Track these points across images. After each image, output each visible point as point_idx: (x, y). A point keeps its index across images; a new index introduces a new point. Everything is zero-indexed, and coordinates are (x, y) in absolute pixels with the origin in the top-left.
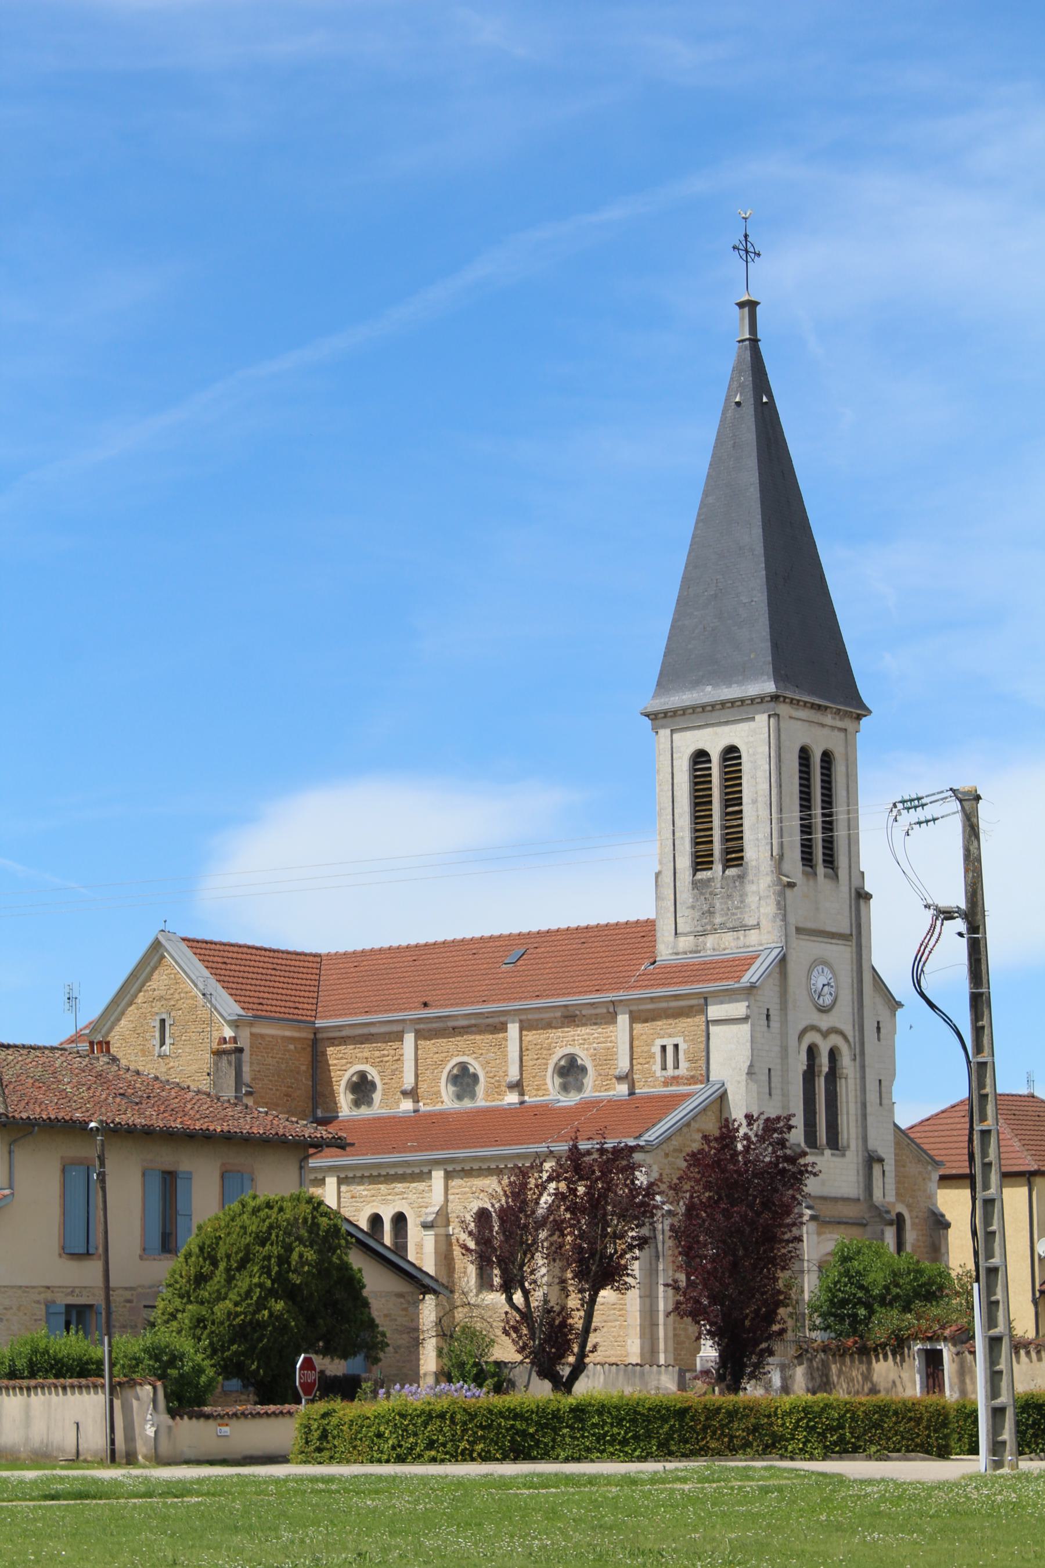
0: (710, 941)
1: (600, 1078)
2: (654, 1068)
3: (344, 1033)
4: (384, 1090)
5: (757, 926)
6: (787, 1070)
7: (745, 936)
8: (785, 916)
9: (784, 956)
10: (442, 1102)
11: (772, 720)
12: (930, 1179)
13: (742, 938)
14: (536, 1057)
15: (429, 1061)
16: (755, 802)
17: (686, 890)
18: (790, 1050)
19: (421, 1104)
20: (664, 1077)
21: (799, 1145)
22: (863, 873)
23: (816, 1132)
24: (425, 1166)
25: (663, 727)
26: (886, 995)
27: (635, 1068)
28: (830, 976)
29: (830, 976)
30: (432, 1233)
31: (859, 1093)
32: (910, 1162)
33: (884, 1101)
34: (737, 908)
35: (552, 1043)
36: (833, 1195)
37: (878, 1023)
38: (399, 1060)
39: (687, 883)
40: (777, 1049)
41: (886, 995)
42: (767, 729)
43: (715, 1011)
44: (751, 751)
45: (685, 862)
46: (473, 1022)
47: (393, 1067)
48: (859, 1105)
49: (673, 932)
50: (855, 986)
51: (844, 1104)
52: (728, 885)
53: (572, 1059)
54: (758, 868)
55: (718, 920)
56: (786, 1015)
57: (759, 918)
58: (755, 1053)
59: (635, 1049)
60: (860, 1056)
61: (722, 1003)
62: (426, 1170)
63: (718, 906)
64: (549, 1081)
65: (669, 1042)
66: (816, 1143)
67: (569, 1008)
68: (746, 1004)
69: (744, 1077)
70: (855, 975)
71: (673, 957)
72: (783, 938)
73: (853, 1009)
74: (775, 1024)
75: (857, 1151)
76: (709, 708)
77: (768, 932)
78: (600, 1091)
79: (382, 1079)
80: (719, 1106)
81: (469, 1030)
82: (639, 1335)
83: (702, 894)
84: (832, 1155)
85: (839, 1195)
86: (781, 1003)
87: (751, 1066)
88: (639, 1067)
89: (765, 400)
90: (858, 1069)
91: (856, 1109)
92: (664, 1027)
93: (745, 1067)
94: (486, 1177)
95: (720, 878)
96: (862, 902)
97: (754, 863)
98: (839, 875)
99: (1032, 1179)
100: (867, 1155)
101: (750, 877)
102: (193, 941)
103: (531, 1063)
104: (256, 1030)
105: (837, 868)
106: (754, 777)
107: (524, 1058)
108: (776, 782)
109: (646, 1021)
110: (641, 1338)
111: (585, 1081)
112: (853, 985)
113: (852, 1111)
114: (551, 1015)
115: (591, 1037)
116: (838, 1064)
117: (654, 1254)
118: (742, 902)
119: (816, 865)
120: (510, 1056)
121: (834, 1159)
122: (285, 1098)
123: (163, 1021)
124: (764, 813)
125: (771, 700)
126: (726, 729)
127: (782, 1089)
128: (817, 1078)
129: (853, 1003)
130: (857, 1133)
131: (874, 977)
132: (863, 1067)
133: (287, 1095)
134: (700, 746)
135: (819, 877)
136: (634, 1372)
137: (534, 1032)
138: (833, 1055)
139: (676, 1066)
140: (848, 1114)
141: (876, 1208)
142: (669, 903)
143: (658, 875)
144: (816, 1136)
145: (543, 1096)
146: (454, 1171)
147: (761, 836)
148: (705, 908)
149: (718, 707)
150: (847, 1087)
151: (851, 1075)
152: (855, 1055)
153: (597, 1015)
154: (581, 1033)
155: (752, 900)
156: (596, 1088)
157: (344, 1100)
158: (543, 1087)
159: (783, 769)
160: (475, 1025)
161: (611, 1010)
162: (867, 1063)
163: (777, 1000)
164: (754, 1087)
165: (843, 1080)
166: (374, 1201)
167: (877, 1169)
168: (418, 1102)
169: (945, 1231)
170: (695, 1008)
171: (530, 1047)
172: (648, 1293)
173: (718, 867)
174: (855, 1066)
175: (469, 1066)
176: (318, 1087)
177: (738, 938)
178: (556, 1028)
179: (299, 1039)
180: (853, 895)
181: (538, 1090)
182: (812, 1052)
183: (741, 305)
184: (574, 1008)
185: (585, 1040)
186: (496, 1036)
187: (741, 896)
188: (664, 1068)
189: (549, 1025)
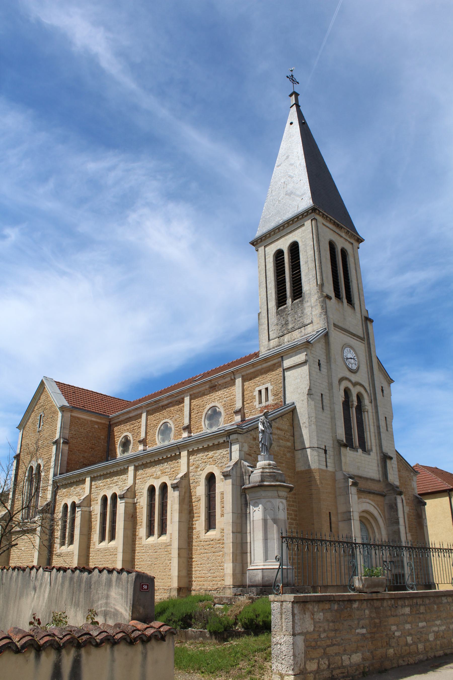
0: (286, 338)
1: (227, 416)
2: (255, 404)
3: (120, 419)
4: (133, 443)
5: (312, 322)
6: (333, 396)
7: (305, 329)
8: (326, 312)
9: (327, 332)
10: (156, 444)
11: (313, 222)
12: (413, 480)
13: (303, 331)
14: (197, 412)
15: (152, 425)
16: (306, 262)
17: (274, 317)
18: (334, 384)
19: (147, 447)
20: (260, 407)
21: (343, 441)
22: (367, 311)
23: (352, 439)
24: (126, 464)
25: (261, 246)
26: (385, 374)
27: (245, 406)
28: (354, 355)
29: (354, 355)
30: (124, 501)
31: (375, 420)
32: (403, 470)
33: (389, 429)
34: (300, 317)
35: (204, 403)
36: (365, 476)
37: (382, 387)
38: (139, 428)
39: (274, 314)
40: (326, 384)
41: (385, 374)
42: (311, 226)
43: (287, 363)
44: (303, 240)
45: (272, 303)
46: (170, 401)
47: (138, 431)
48: (376, 427)
49: (267, 339)
50: (368, 364)
51: (367, 426)
52: (294, 307)
53: (214, 409)
54: (310, 294)
55: (290, 326)
56: (330, 365)
57: (312, 319)
58: (312, 382)
59: (245, 396)
60: (374, 401)
61: (291, 357)
62: (126, 467)
63: (290, 319)
64: (203, 423)
65: (263, 388)
66: (353, 446)
67: (212, 382)
68: (305, 353)
69: (306, 397)
70: (368, 358)
71: (267, 352)
72: (326, 325)
73: (368, 376)
74: (324, 369)
75: (377, 453)
76: (282, 228)
77: (318, 323)
78: (227, 423)
79: (133, 438)
80: (291, 416)
81: (169, 406)
82: (231, 561)
83: (281, 316)
84: (363, 453)
85: (368, 477)
86: (327, 359)
87: (310, 389)
88: (247, 405)
89: (303, 121)
90: (373, 407)
91: (374, 429)
92: (260, 380)
93: (306, 391)
94: (154, 466)
95: (290, 306)
96: (369, 323)
97: (308, 292)
98: (355, 307)
99: (450, 493)
100: (382, 455)
101: (306, 299)
102: (59, 383)
103: (195, 416)
104: (73, 414)
105: (354, 304)
106: (306, 251)
107: (192, 414)
108: (317, 249)
109: (251, 379)
110: (233, 562)
111: (220, 420)
112: (367, 364)
113: (372, 430)
114: (204, 388)
115: (223, 395)
116: (362, 404)
117: (243, 502)
118: (302, 313)
119: (342, 298)
120: (185, 413)
121: (364, 455)
122: (91, 450)
123: (41, 415)
124: (312, 265)
125: (312, 212)
126: (290, 235)
127: (330, 408)
128: (351, 409)
129: (368, 373)
130: (376, 443)
131: (378, 363)
132: (376, 407)
133: (91, 448)
134: (278, 248)
135: (344, 304)
136: (80, 580)
137: (196, 399)
138: (359, 397)
139: (267, 400)
140: (370, 432)
141: (391, 485)
142: (265, 325)
143: (259, 314)
144: (352, 442)
145: (199, 432)
146: (139, 466)
147: (311, 277)
148: (283, 322)
149: (286, 226)
150: (368, 417)
151: (370, 411)
152: (371, 400)
153: (226, 382)
154: (218, 395)
155: (308, 310)
156: (225, 422)
157: (119, 450)
158: (200, 427)
159: (321, 244)
160: (171, 403)
161: (233, 377)
162: (378, 405)
163: (325, 357)
164: (313, 403)
165: (366, 413)
166: (104, 488)
167: (388, 462)
168: (146, 446)
169: (424, 507)
170: (277, 365)
171: (194, 408)
172: (239, 530)
173: (289, 301)
174: (372, 406)
175: (168, 424)
176: (110, 447)
177: (301, 332)
178: (206, 395)
179: (101, 423)
180: (363, 319)
181: (197, 429)
182: (347, 392)
183: (291, 95)
184: (215, 381)
185: (220, 397)
186: (180, 406)
187: (302, 310)
188: (260, 402)
189: (203, 394)
